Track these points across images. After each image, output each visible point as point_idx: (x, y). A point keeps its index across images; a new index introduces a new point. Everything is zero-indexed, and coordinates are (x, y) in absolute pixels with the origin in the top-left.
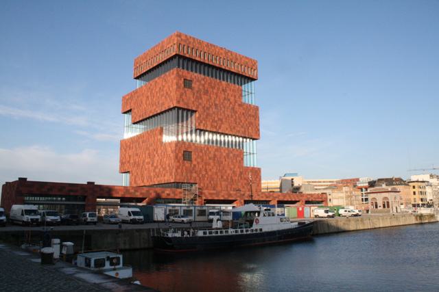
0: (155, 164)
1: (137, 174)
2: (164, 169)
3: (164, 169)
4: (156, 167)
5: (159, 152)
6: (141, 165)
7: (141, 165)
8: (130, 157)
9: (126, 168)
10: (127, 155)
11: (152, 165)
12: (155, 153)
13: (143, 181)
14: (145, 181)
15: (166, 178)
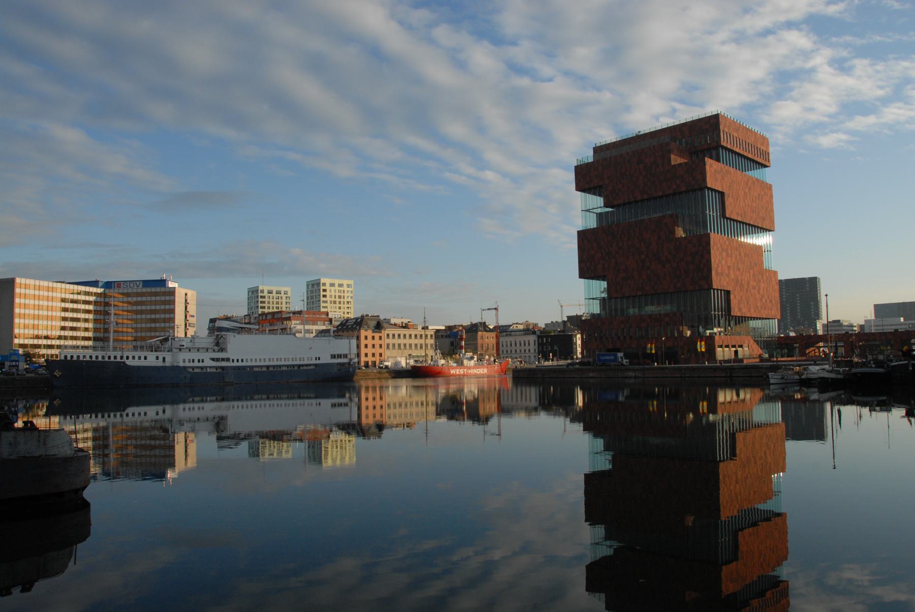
0: (761, 291)
1: (741, 297)
2: (771, 301)
3: (771, 301)
4: (763, 296)
5: (764, 277)
6: (746, 287)
7: (746, 287)
8: (729, 267)
9: (725, 284)
10: (723, 262)
11: (759, 293)
12: (760, 276)
13: (749, 311)
14: (752, 310)
15: (773, 313)
